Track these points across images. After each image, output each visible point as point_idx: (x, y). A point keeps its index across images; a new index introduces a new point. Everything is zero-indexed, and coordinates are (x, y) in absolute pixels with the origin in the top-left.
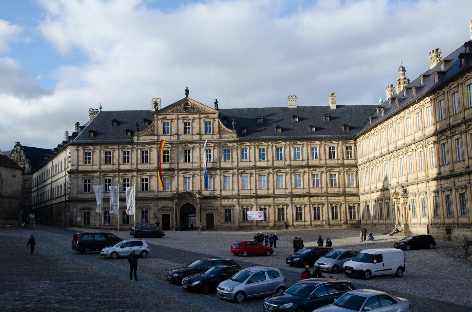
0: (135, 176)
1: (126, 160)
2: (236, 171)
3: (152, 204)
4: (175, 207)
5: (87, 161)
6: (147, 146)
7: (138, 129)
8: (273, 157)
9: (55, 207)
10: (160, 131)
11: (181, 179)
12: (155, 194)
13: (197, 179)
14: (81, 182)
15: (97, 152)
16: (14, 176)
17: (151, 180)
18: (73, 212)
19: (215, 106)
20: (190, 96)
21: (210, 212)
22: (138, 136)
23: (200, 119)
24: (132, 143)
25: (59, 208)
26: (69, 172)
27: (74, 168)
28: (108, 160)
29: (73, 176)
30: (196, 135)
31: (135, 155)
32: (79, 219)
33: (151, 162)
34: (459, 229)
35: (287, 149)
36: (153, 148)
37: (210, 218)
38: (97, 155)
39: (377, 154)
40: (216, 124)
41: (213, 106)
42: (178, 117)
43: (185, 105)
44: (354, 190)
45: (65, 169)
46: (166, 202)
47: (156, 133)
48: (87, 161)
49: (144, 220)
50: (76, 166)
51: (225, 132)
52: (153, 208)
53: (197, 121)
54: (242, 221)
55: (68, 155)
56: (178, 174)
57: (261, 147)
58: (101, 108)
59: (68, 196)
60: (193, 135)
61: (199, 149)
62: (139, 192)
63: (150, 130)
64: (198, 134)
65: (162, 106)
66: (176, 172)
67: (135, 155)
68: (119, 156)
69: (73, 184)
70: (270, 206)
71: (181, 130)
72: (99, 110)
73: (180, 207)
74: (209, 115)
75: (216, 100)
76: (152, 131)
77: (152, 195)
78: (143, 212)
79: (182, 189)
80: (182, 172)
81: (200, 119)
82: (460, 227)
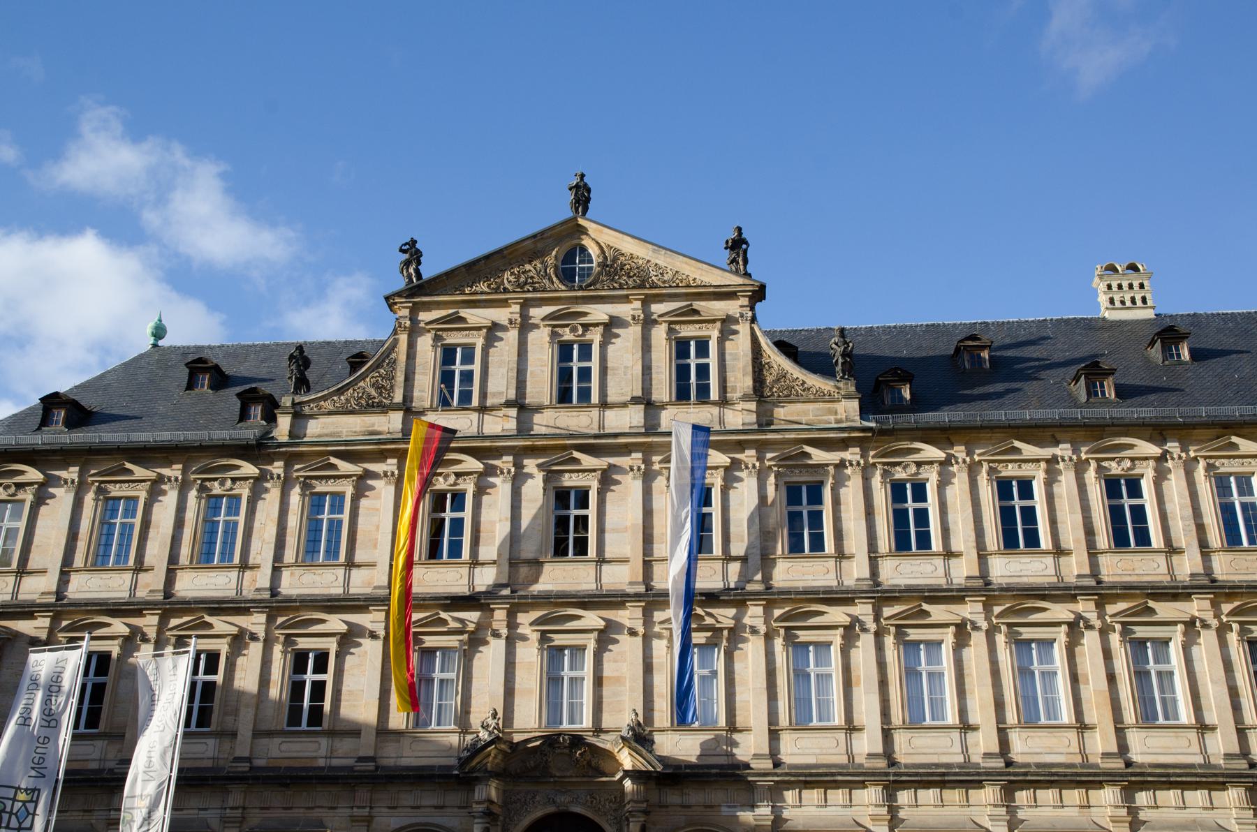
0: (254, 637)
2: (863, 610)
6: (344, 467)
8: (1090, 532)
11: (529, 654)
12: (366, 746)
13: (624, 658)
15: (62, 498)
17: (349, 661)
23: (648, 323)
24: (259, 450)
30: (624, 405)
33: (359, 557)
35: (1175, 485)
36: (375, 476)
42: (524, 316)
43: (569, 257)
46: (429, 799)
47: (398, 397)
51: (791, 395)
53: (629, 338)
56: (512, 625)
57: (1010, 471)
60: (604, 405)
61: (638, 484)
62: (269, 734)
63: (366, 384)
64: (635, 401)
66: (500, 615)
68: (179, 524)
71: (541, 385)
74: (698, 305)
75: (739, 229)
76: (376, 386)
77: (344, 754)
79: (528, 719)
80: (536, 614)
81: (648, 323)
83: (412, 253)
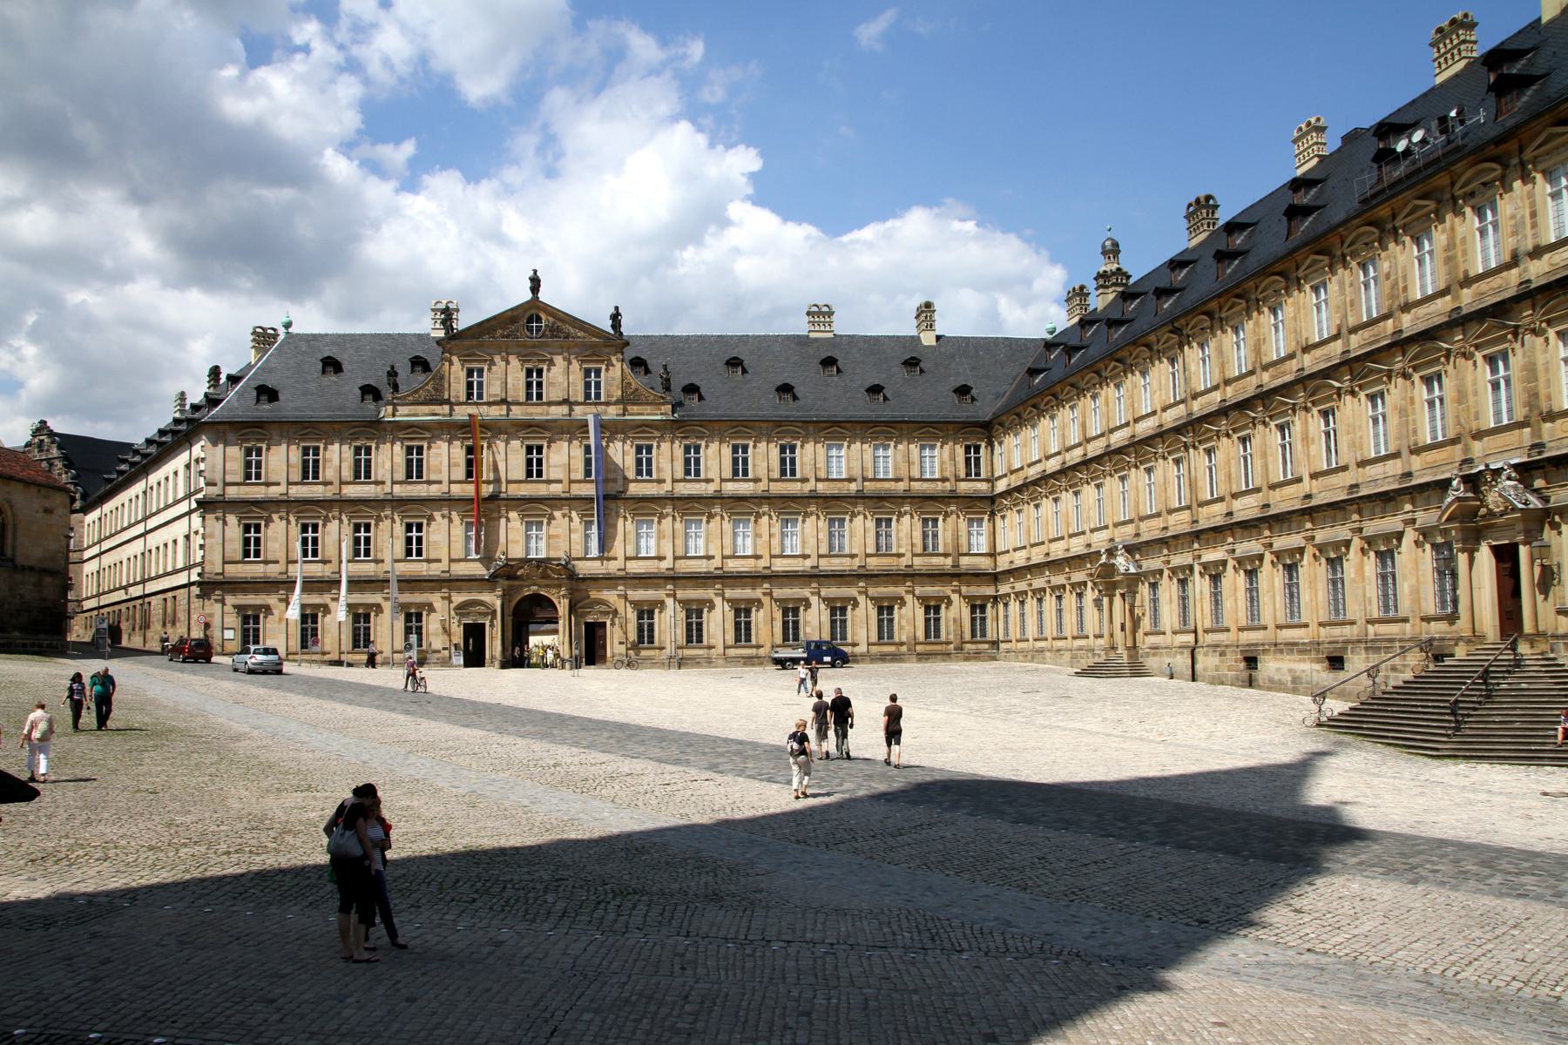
1: (362, 471)
3: (436, 599)
4: (498, 603)
5: (252, 472)
7: (396, 388)
9: (156, 601)
10: (458, 389)
16: (48, 511)
18: (211, 615)
19: (613, 327)
20: (544, 296)
22: (395, 405)
25: (169, 604)
27: (214, 491)
32: (229, 634)
34: (1279, 656)
39: (1053, 465)
41: (606, 325)
44: (985, 564)
48: (252, 472)
49: (413, 638)
50: (220, 484)
58: (288, 325)
59: (199, 570)
65: (463, 322)
69: (212, 536)
70: (759, 601)
72: (282, 332)
73: (514, 603)
77: (435, 570)
78: (408, 617)
82: (1281, 651)
83: (447, 315)
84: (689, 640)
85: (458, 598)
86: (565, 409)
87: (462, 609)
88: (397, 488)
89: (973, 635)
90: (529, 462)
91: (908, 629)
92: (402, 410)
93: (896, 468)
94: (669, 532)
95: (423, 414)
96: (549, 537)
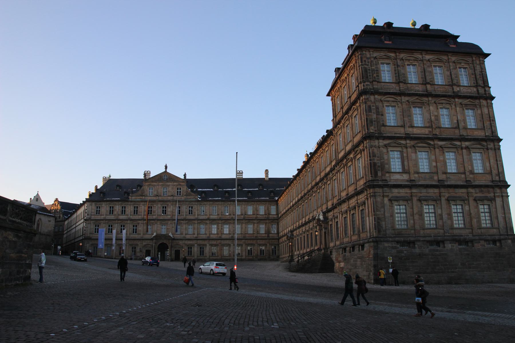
3: (139, 243)
5: (98, 212)
14: (93, 227)
20: (168, 171)
21: (177, 249)
24: (127, 201)
26: (85, 220)
28: (111, 212)
29: (87, 222)
31: (130, 209)
37: (177, 253)
38: (105, 208)
40: (184, 188)
41: (183, 177)
45: (84, 217)
46: (149, 241)
48: (98, 212)
52: (140, 245)
54: (199, 255)
55: (86, 208)
67: (130, 209)
84: (201, 255)
85: (144, 243)
86: (172, 198)
87: (145, 246)
88: (131, 216)
89: (273, 254)
90: (163, 210)
91: (256, 252)
92: (133, 198)
93: (253, 212)
94: (196, 228)
95: (138, 199)
96: (167, 229)
